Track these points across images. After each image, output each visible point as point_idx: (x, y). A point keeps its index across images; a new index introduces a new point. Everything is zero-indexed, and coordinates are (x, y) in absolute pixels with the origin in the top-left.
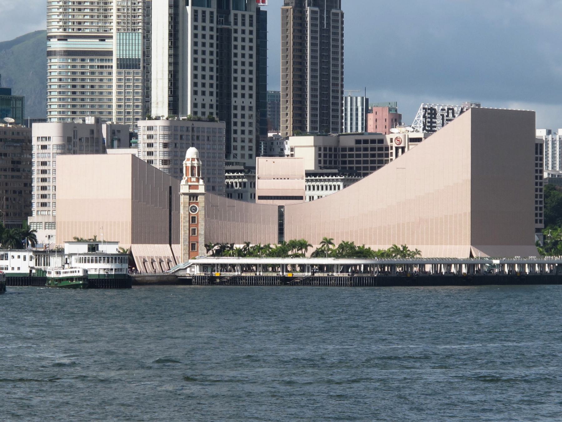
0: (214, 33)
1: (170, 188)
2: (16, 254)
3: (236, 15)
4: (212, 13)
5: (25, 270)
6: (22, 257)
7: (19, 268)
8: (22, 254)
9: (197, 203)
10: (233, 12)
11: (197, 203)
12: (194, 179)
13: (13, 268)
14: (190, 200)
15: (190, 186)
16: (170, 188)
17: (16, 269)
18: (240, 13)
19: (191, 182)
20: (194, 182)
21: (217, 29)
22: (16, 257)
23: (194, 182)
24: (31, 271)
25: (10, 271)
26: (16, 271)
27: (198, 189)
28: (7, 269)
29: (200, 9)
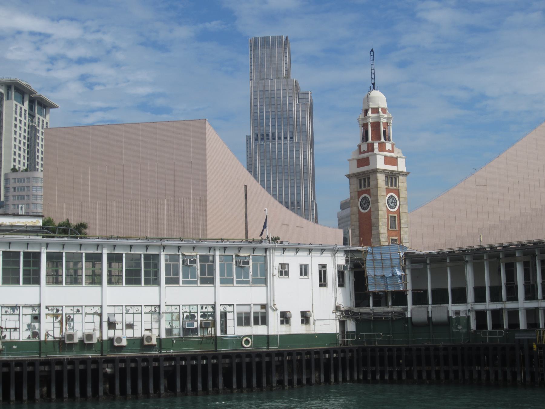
0: (27, 128)
1: (246, 186)
2: (295, 261)
3: (39, 119)
4: (25, 111)
5: (325, 323)
6: (314, 272)
7: (305, 318)
8: (315, 261)
9: (398, 192)
10: (37, 116)
13: (285, 318)
15: (386, 157)
16: (246, 186)
17: (296, 319)
18: (41, 118)
20: (389, 151)
21: (29, 125)
22: (294, 270)
24: (342, 324)
25: (275, 327)
26: (296, 327)
28: (262, 319)
29: (19, 105)
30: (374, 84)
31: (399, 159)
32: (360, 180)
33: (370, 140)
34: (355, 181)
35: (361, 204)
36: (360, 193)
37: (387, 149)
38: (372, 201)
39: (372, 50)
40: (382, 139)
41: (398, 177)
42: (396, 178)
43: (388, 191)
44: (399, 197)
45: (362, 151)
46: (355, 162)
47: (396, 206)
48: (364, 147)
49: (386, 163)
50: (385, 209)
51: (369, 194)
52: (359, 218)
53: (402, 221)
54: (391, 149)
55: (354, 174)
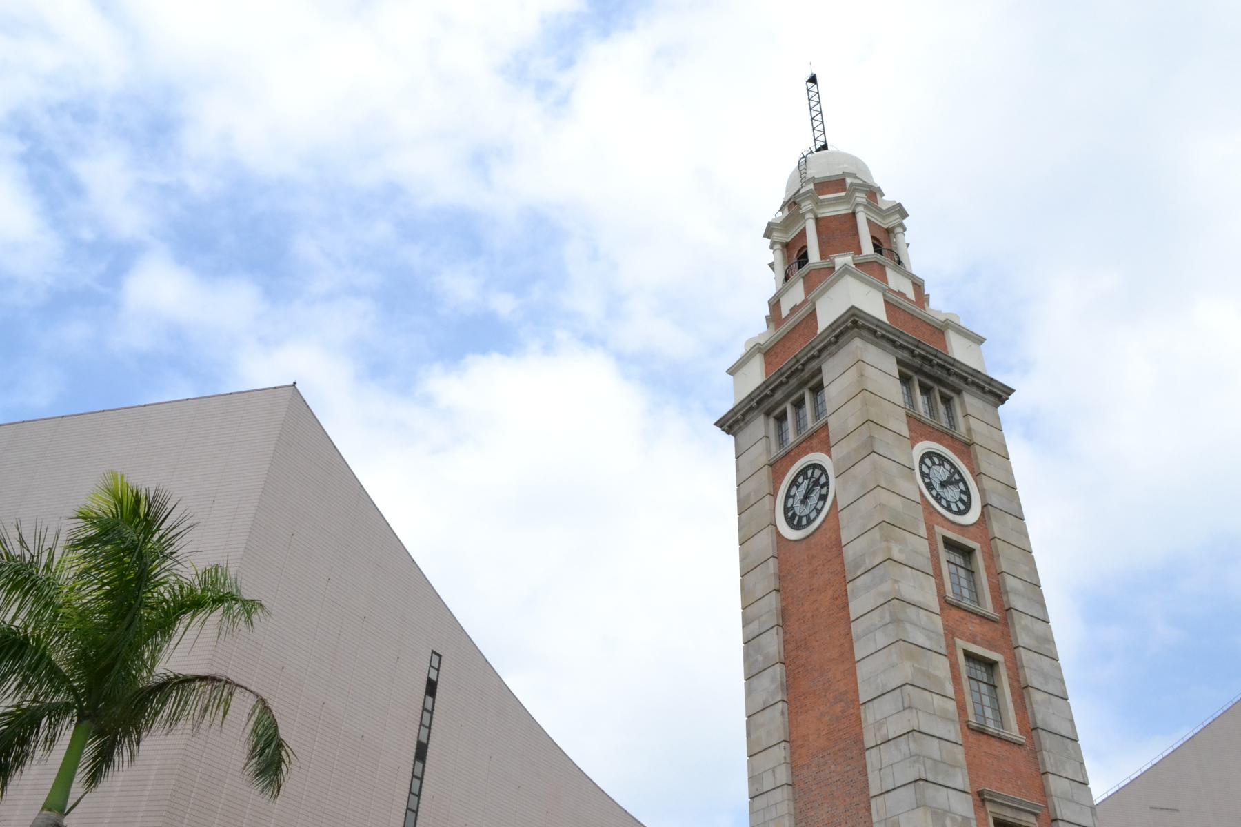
33: (814, 256)
34: (760, 426)
36: (777, 467)
38: (836, 466)
40: (868, 248)
41: (959, 392)
42: (947, 401)
44: (977, 475)
45: (785, 311)
47: (968, 505)
48: (797, 294)
50: (919, 499)
52: (781, 578)
53: (1011, 582)
54: (911, 294)
55: (750, 397)
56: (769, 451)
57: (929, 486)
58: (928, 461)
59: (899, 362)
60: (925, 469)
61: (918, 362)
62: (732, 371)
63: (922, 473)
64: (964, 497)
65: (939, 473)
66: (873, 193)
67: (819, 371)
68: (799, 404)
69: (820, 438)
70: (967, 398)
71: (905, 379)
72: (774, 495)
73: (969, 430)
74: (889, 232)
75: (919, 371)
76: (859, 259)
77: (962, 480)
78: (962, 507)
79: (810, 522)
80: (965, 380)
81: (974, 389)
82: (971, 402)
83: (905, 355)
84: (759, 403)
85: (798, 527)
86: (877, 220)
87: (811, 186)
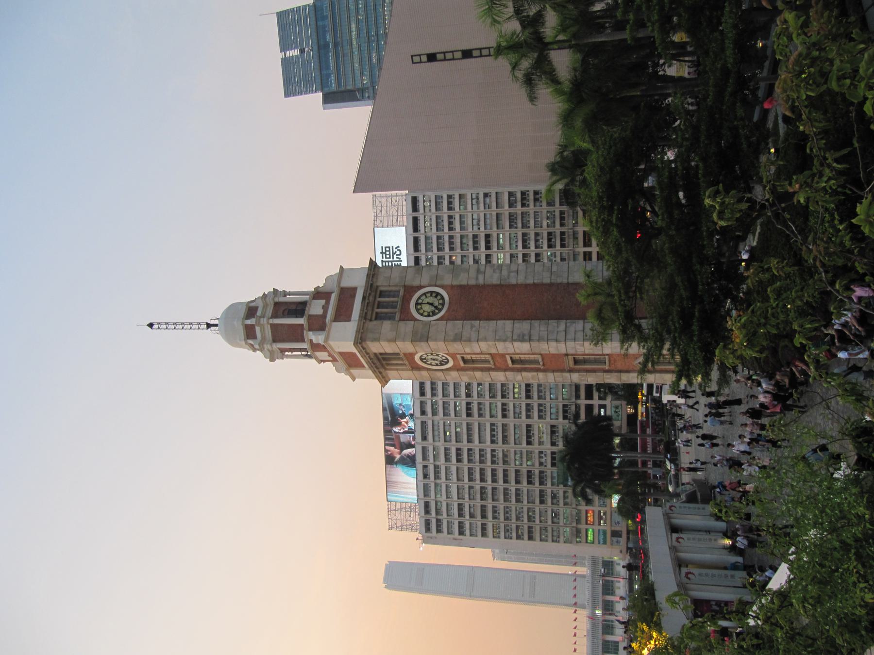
9: (410, 290)
11: (410, 290)
12: (316, 308)
14: (390, 317)
19: (324, 316)
23: (325, 308)
27: (354, 290)
30: (209, 326)
31: (346, 283)
32: (388, 364)
35: (437, 365)
37: (320, 312)
39: (151, 325)
41: (377, 287)
42: (382, 294)
43: (406, 316)
44: (420, 287)
46: (354, 371)
47: (438, 294)
48: (323, 355)
49: (348, 319)
51: (415, 354)
54: (323, 302)
56: (402, 370)
57: (434, 314)
58: (421, 311)
59: (371, 320)
60: (426, 314)
61: (370, 308)
62: (354, 379)
63: (428, 316)
64: (434, 295)
65: (427, 308)
66: (251, 311)
67: (375, 354)
68: (384, 359)
69: (410, 357)
70: (379, 283)
71: (379, 317)
72: (428, 369)
73: (396, 286)
74: (276, 304)
75: (373, 310)
76: (306, 327)
77: (425, 294)
78: (439, 297)
79: (447, 359)
80: (372, 285)
81: (374, 280)
82: (381, 282)
83: (369, 317)
84: (380, 373)
85: (447, 362)
86: (270, 311)
87: (250, 341)
